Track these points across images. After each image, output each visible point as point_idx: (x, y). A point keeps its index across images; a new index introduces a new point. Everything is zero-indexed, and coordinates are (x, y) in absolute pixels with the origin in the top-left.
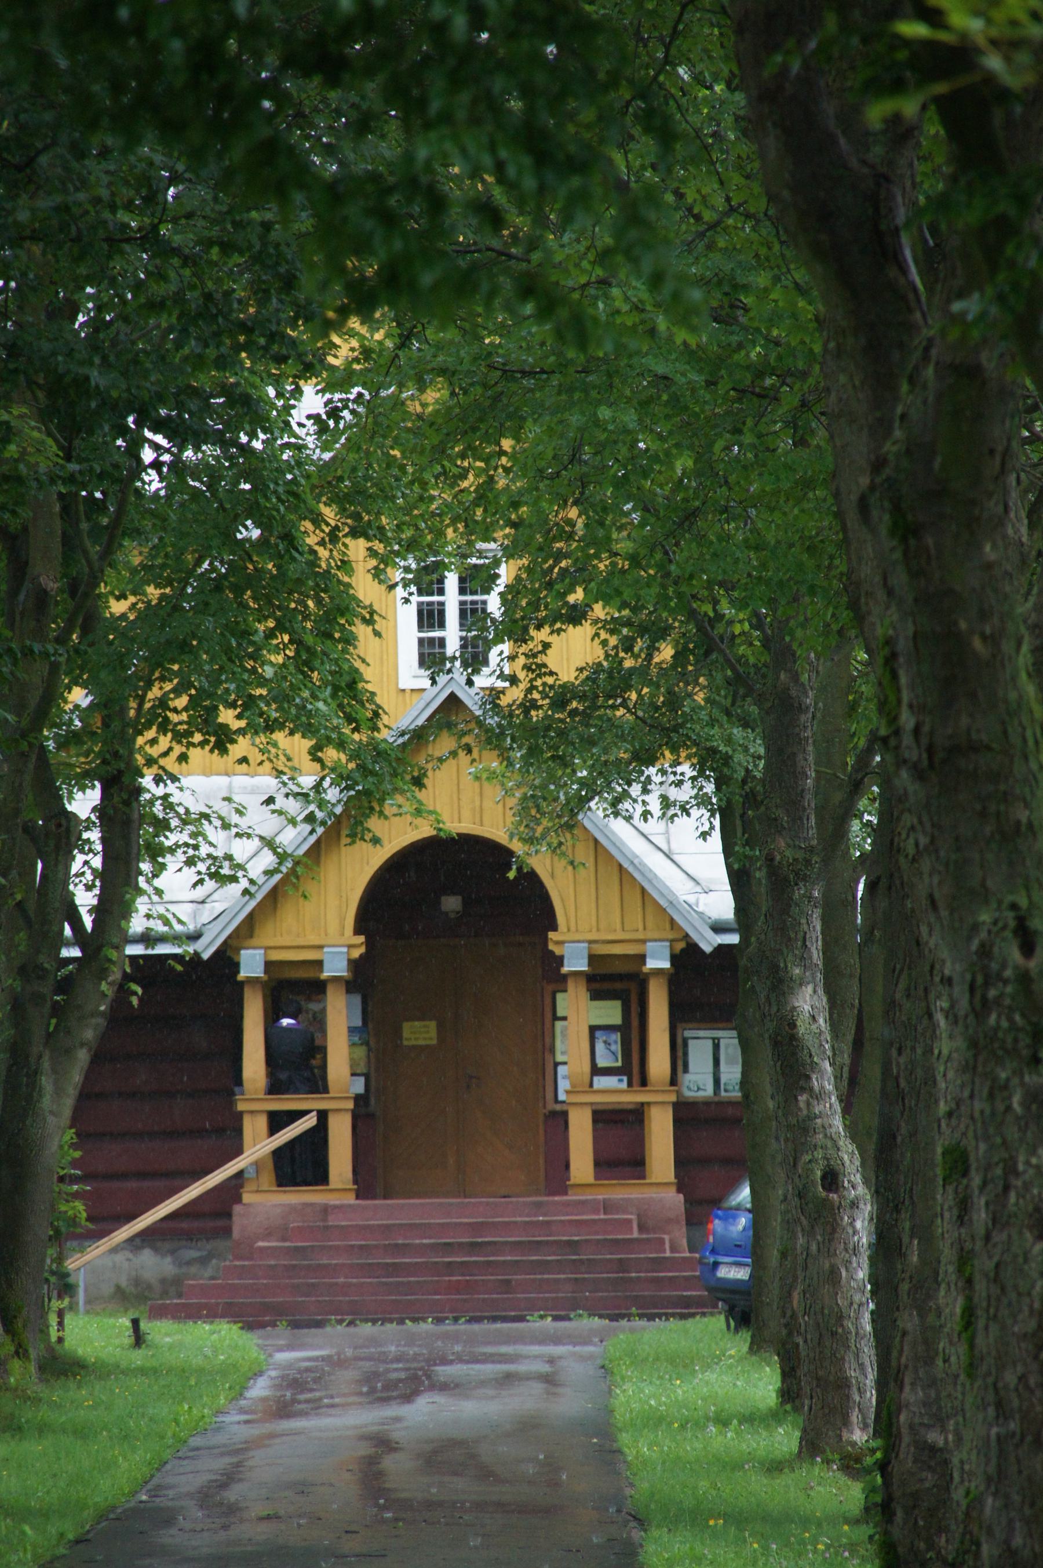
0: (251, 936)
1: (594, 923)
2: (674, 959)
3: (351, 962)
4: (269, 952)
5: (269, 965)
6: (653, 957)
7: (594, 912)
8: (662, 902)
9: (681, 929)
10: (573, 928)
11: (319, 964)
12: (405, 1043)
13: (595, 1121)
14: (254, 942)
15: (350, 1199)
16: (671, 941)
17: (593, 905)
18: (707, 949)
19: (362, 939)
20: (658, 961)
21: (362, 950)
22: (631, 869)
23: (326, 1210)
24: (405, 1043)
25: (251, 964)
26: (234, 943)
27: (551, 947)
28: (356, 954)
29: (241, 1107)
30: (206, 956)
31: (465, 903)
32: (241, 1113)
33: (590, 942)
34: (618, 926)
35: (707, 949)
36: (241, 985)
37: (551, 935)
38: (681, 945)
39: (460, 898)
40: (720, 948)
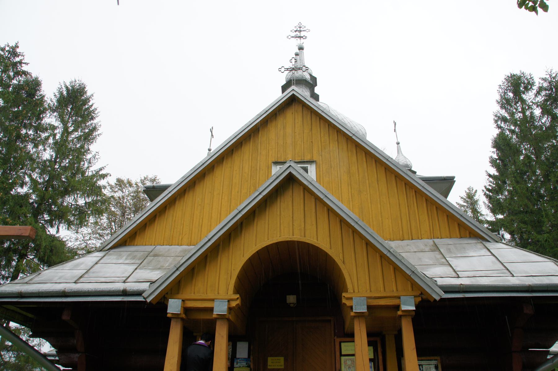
0: (178, 293)
1: (368, 287)
4: (187, 302)
5: (187, 310)
6: (405, 304)
7: (368, 281)
8: (408, 272)
9: (420, 288)
10: (356, 291)
12: (269, 367)
14: (180, 296)
16: (415, 297)
17: (367, 278)
19: (238, 296)
20: (408, 306)
22: (388, 255)
24: (269, 367)
25: (174, 306)
27: (344, 301)
28: (234, 304)
30: (148, 300)
31: (298, 300)
33: (367, 297)
34: (382, 289)
36: (169, 320)
38: (419, 299)
39: (295, 296)
40: (442, 300)
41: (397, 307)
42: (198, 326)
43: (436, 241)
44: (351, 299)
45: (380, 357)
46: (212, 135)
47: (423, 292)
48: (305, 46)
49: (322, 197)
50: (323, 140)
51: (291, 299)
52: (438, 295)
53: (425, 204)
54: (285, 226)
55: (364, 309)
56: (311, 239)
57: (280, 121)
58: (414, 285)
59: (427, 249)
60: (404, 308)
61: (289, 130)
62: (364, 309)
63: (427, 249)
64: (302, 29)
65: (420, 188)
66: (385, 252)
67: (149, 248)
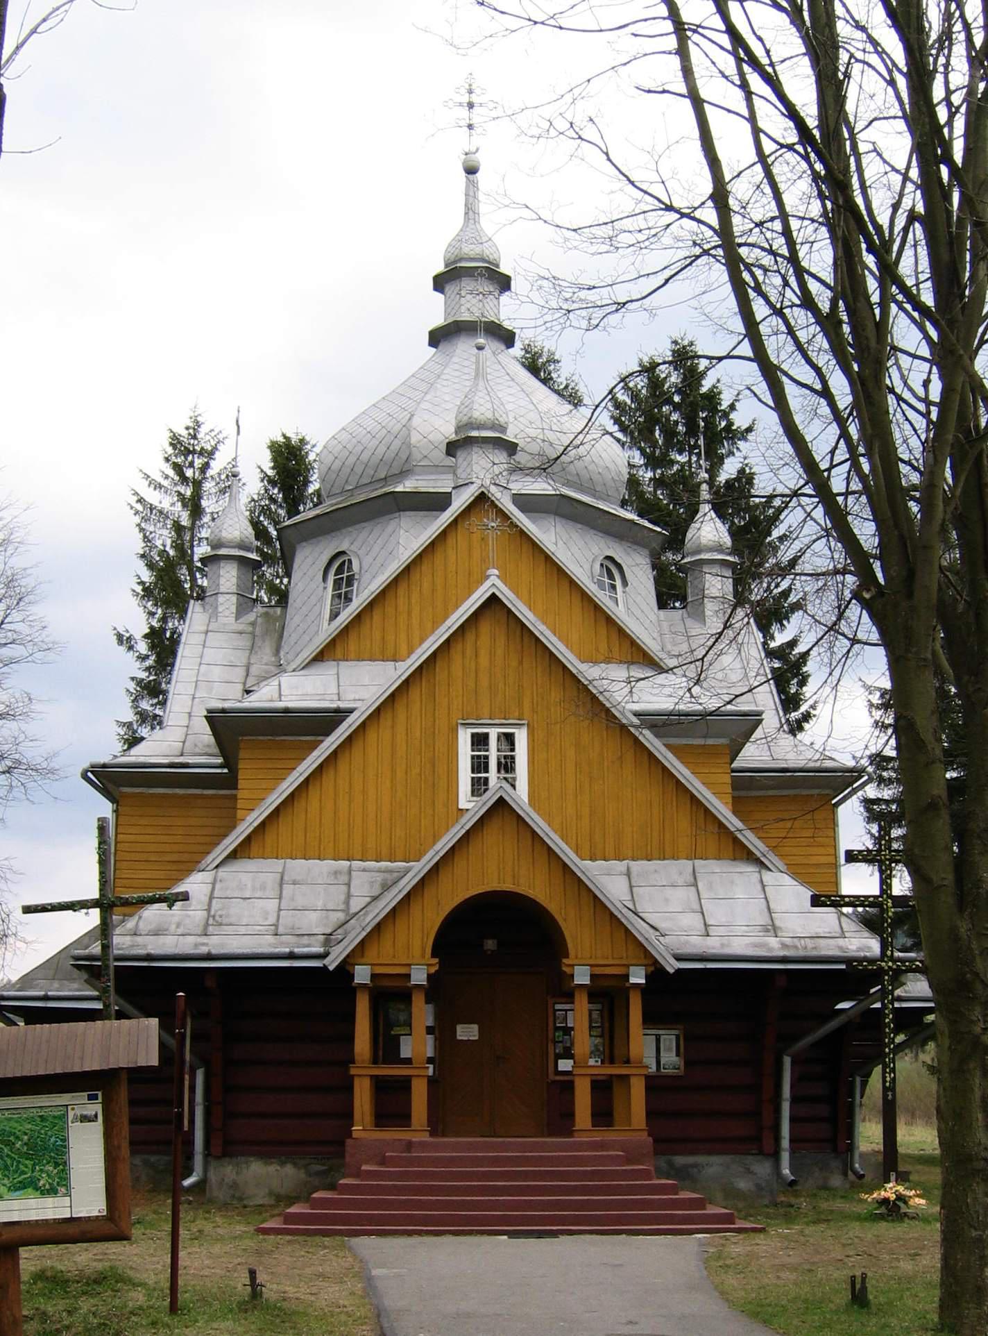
2: (647, 977)
3: (429, 975)
5: (374, 976)
8: (640, 939)
11: (408, 976)
13: (592, 1088)
15: (425, 1137)
18: (671, 971)
19: (437, 960)
20: (638, 977)
21: (437, 968)
23: (409, 1145)
25: (362, 974)
26: (351, 961)
27: (564, 969)
28: (433, 970)
29: (353, 1072)
30: (331, 968)
32: (353, 1076)
33: (591, 966)
35: (671, 971)
37: (565, 961)
38: (652, 969)
40: (679, 971)
41: (626, 977)
42: (391, 996)
43: (698, 862)
44: (573, 966)
45: (607, 1025)
46: (238, 433)
47: (656, 962)
48: (482, 159)
49: (542, 835)
50: (539, 682)
51: (490, 944)
52: (672, 966)
53: (689, 806)
54: (497, 870)
55: (586, 981)
56: (523, 889)
57: (470, 637)
58: (647, 953)
59: (680, 882)
60: (633, 980)
61: (484, 660)
62: (586, 981)
63: (680, 882)
64: (474, 98)
65: (683, 781)
66: (616, 913)
67: (277, 865)
